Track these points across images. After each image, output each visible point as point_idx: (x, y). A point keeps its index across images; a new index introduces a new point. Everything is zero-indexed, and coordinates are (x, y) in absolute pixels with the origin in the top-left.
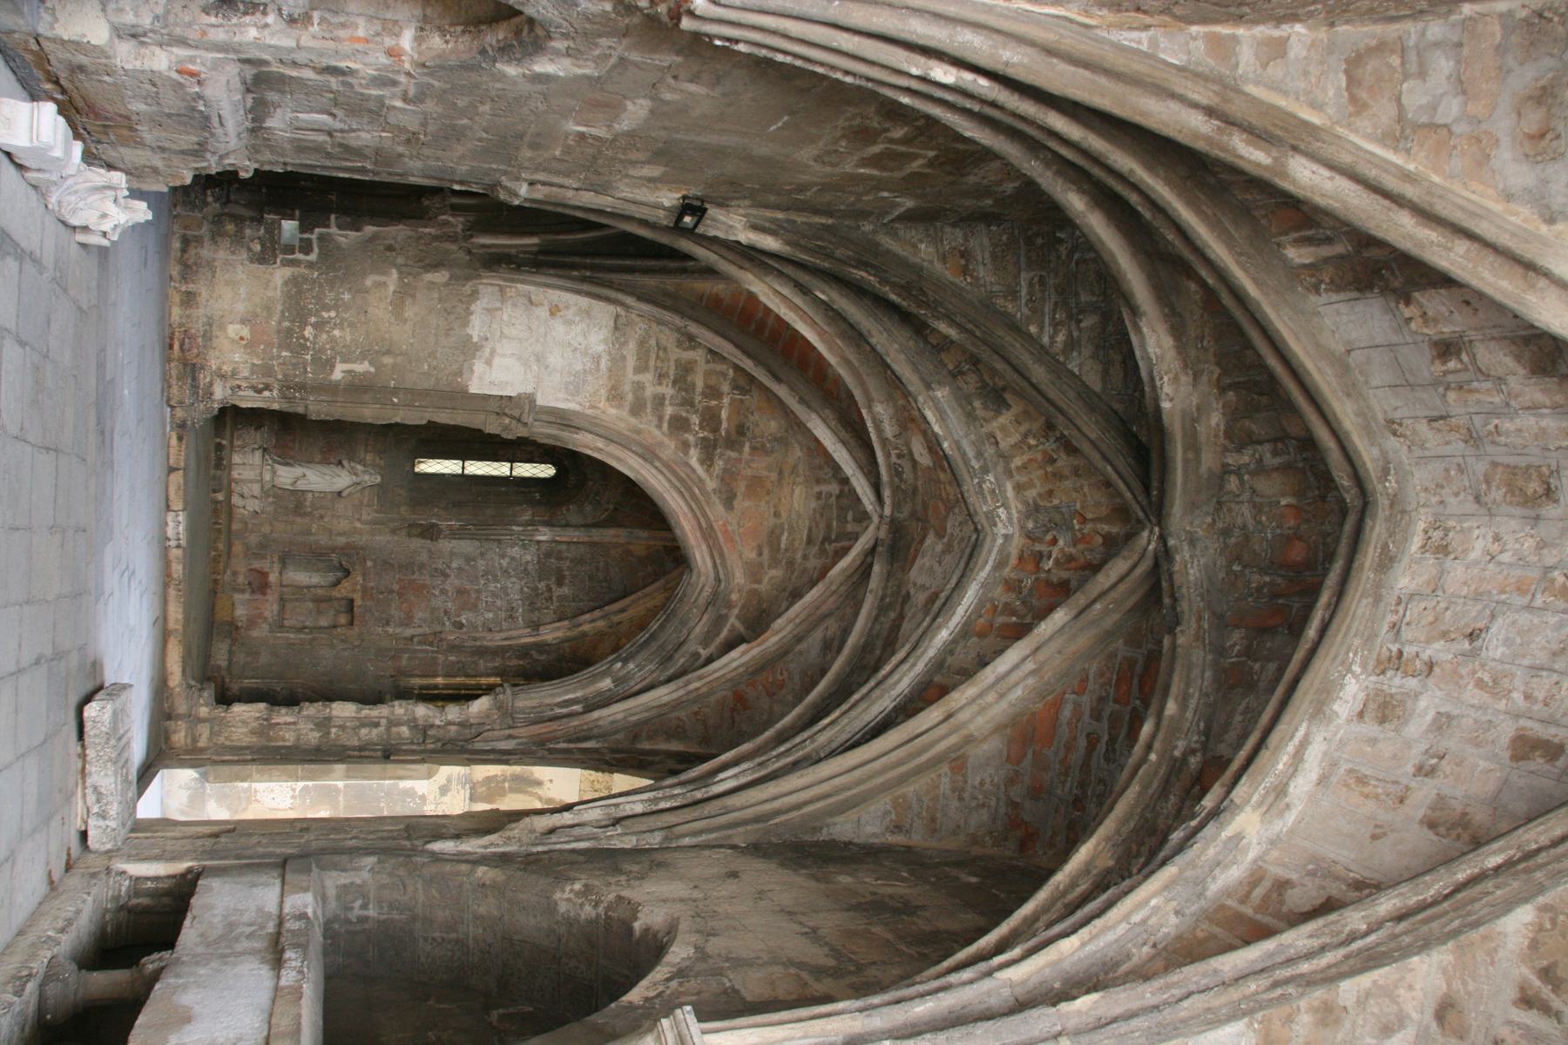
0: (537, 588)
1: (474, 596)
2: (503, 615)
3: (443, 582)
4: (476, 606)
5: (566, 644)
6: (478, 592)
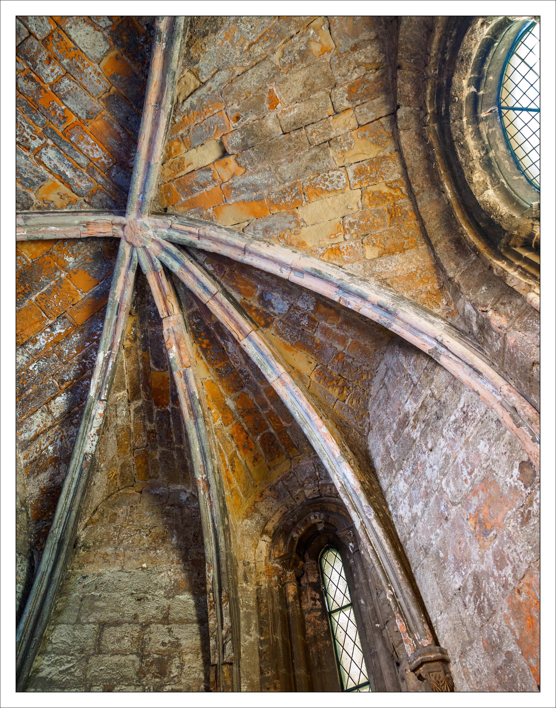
0: (423, 434)
1: (475, 501)
2: (471, 430)
3: (488, 575)
4: (484, 480)
5: (436, 311)
6: (465, 501)
